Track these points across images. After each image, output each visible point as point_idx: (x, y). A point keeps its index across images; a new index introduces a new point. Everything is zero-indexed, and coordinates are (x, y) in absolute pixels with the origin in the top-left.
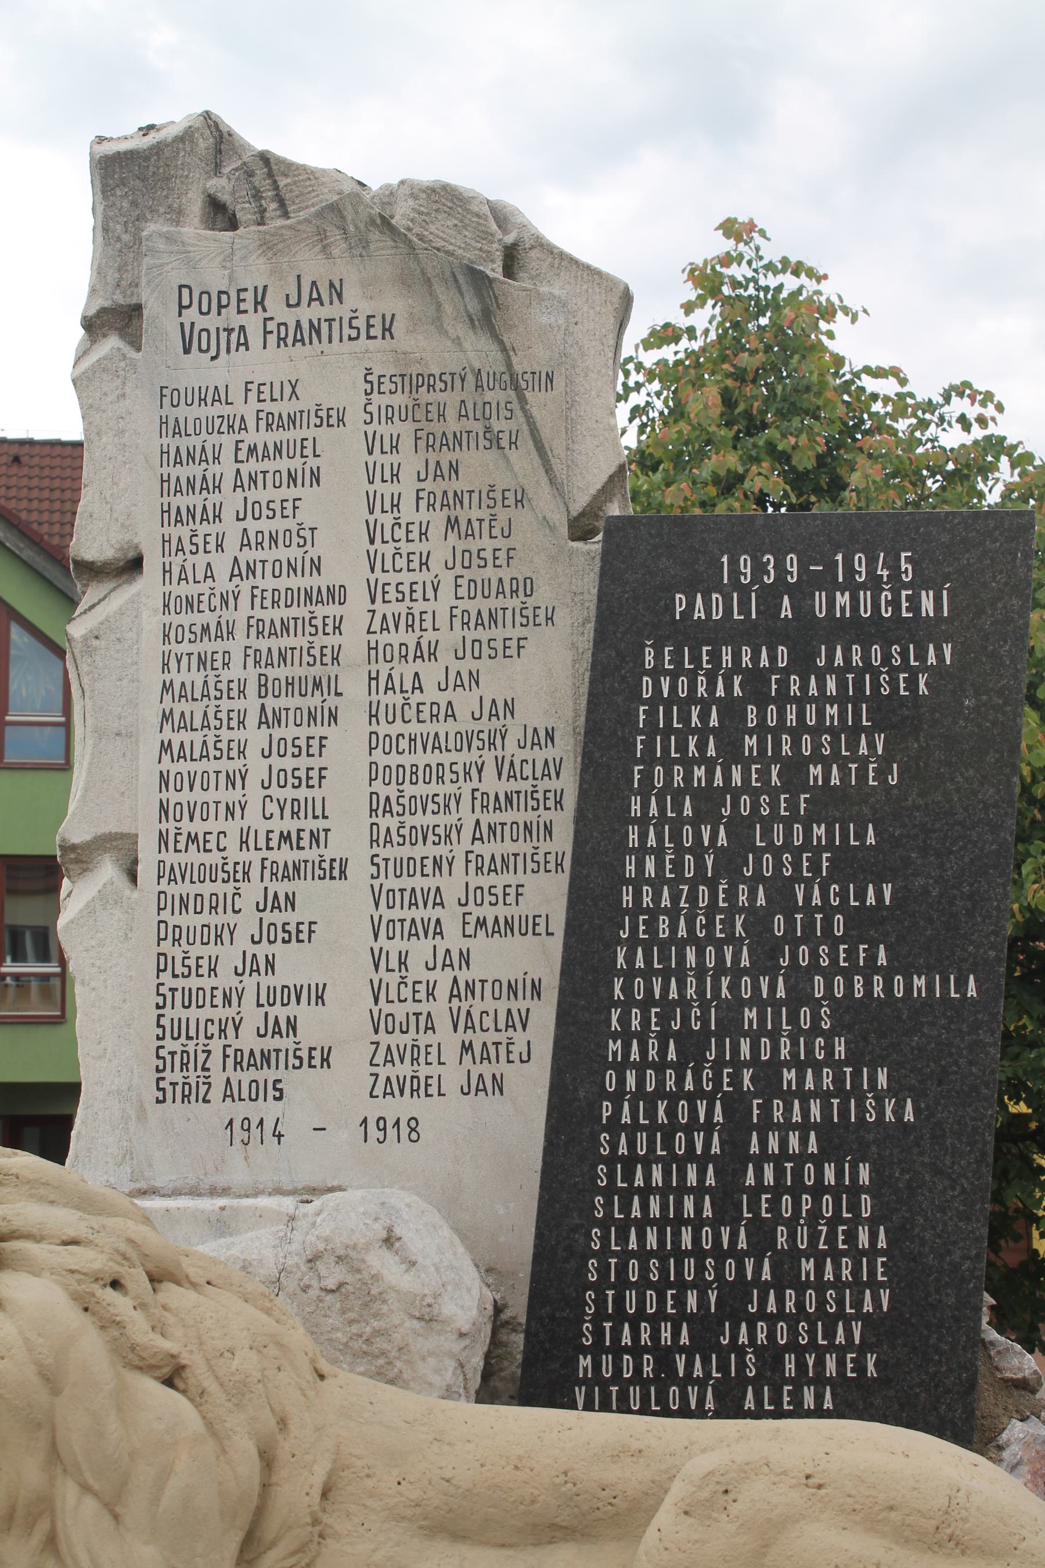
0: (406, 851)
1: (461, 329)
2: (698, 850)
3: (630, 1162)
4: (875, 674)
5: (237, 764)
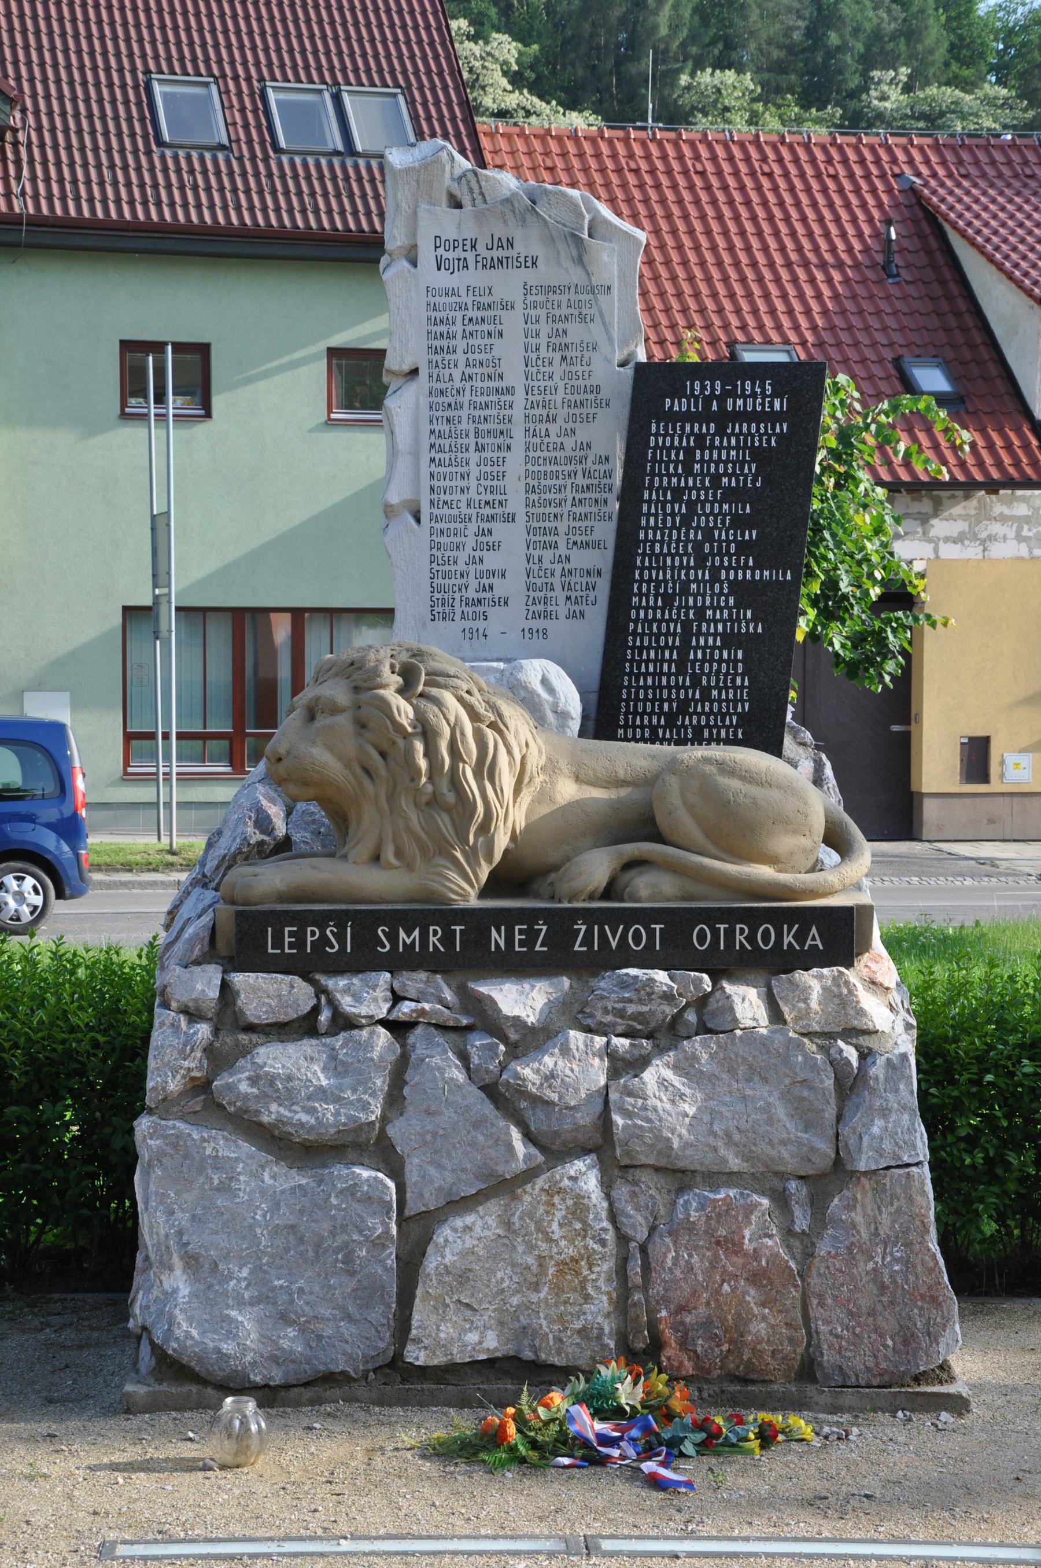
0: (541, 510)
1: (567, 263)
2: (673, 515)
3: (641, 649)
4: (753, 436)
5: (465, 469)
